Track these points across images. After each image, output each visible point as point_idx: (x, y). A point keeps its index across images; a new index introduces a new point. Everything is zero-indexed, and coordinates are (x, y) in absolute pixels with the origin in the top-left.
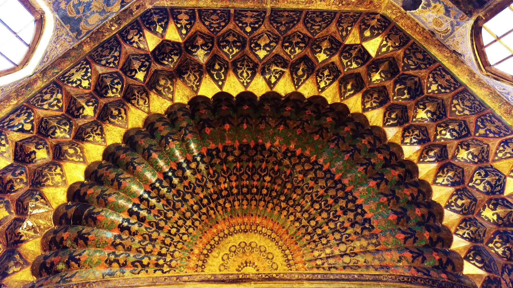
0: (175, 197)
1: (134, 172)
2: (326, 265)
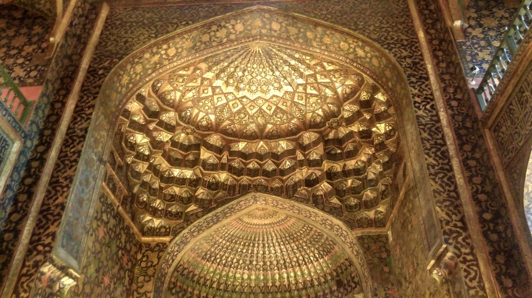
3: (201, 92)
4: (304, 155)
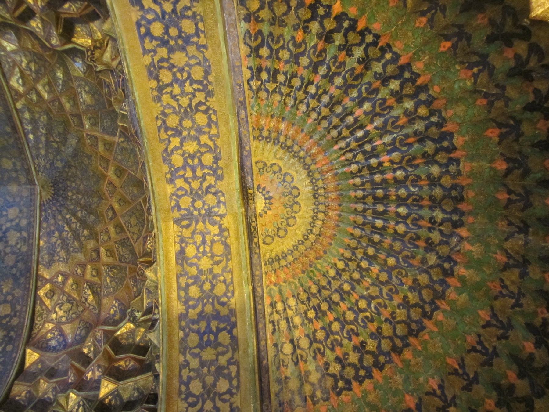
0: (366, 86)
1: (416, 13)
2: (276, 317)
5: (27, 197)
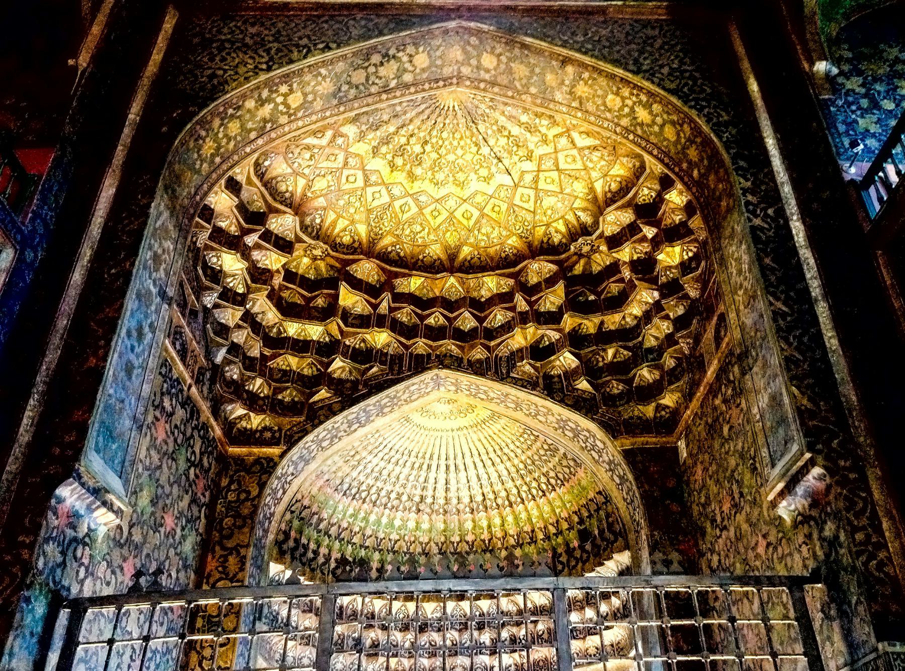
3: (344, 180)
4: (529, 303)
5: (441, 73)
